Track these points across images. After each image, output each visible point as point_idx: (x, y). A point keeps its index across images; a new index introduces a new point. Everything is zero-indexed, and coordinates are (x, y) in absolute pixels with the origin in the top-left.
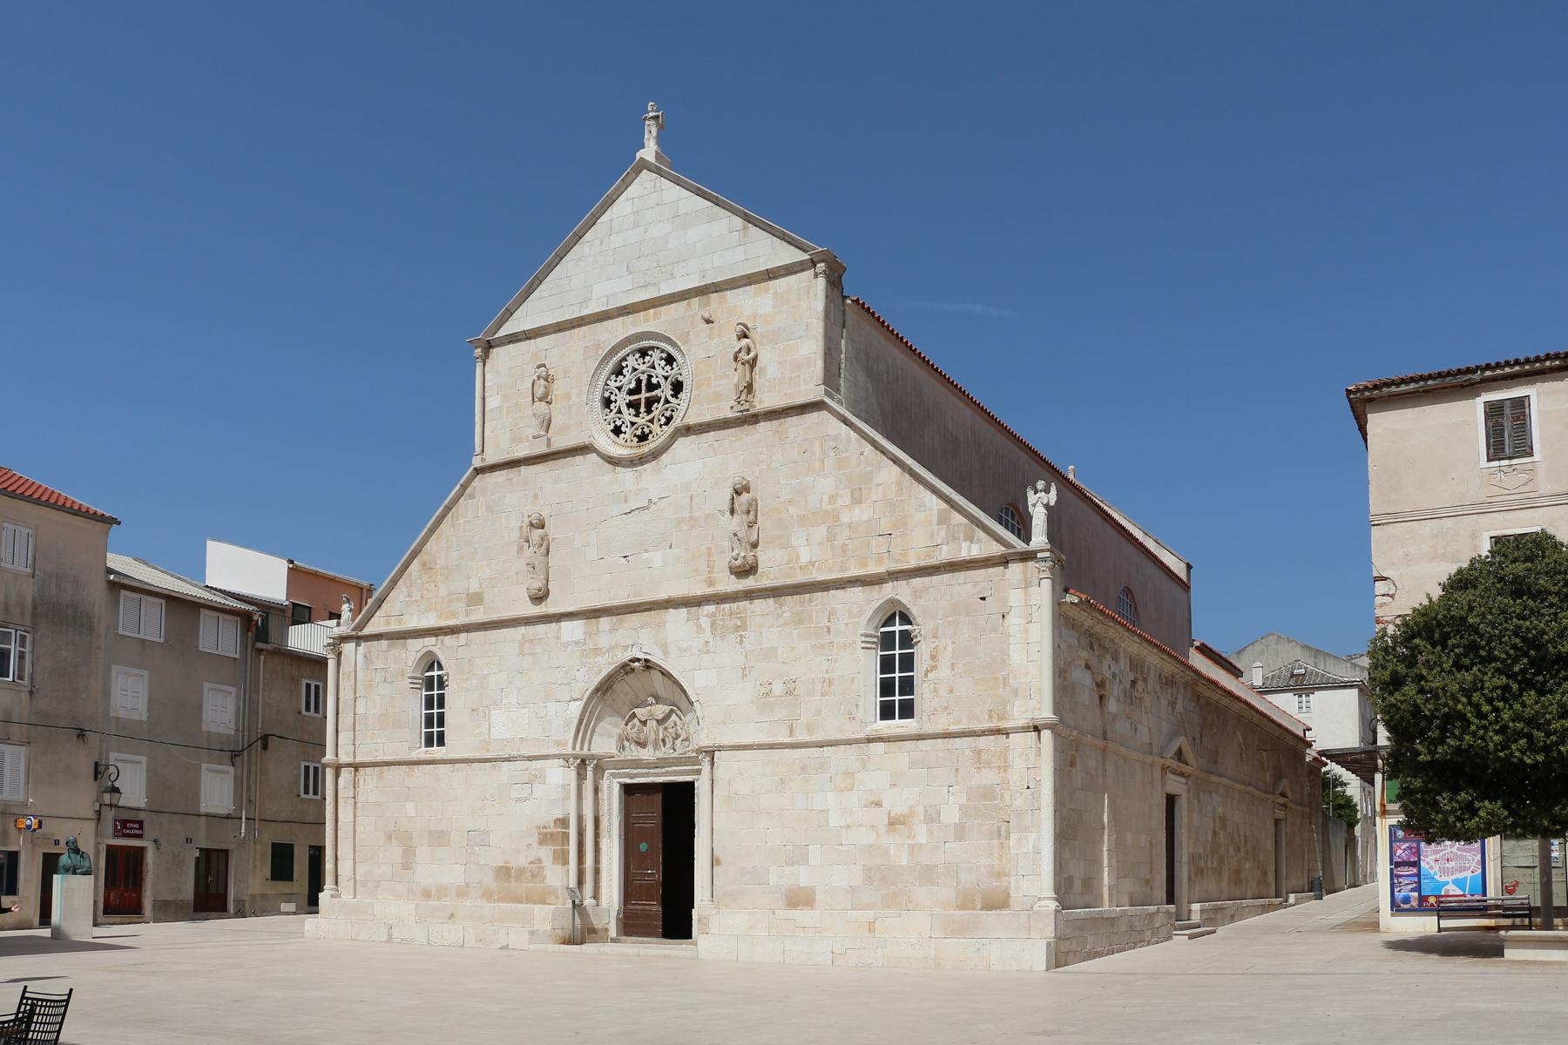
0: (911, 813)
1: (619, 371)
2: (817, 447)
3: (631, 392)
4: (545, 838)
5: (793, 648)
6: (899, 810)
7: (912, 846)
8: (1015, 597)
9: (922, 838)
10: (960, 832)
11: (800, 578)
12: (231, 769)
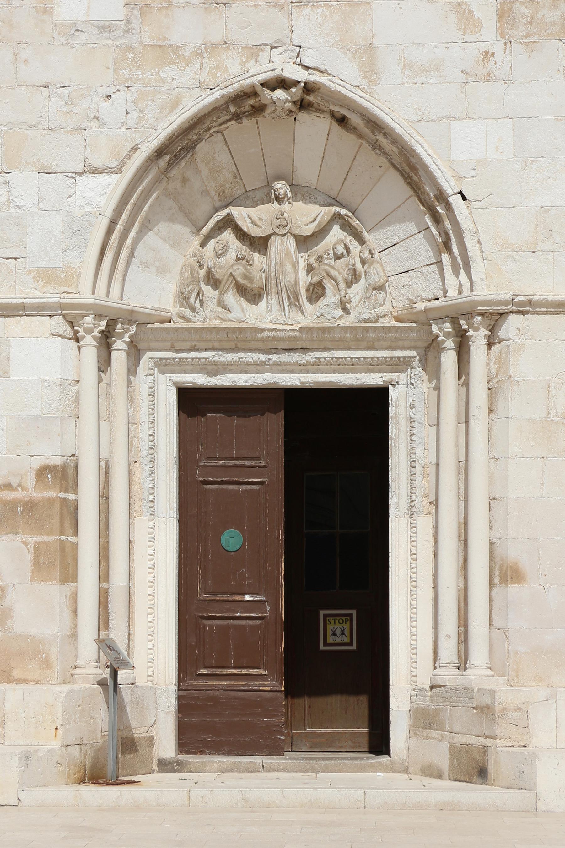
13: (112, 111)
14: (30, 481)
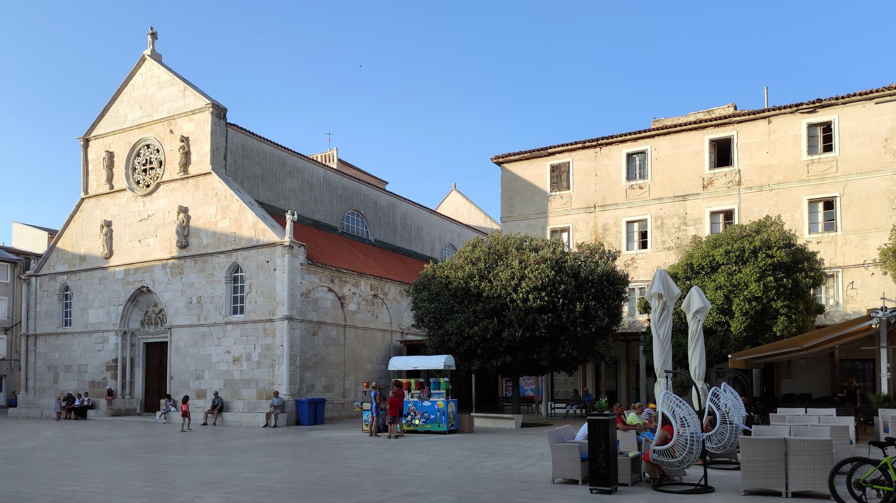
0: (241, 356)
1: (138, 155)
2: (210, 193)
3: (144, 165)
4: (109, 368)
6: (237, 355)
8: (279, 262)
9: (245, 367)
10: (259, 365)
11: (203, 252)
12: (5, 337)
13: (122, 294)
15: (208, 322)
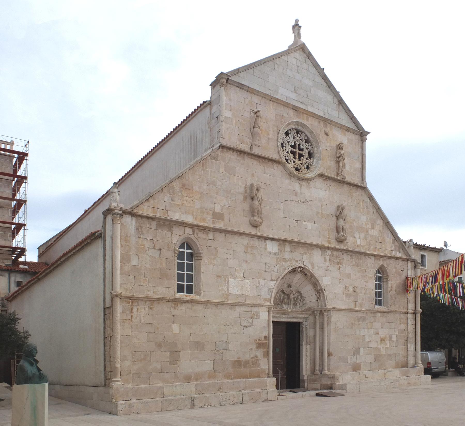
0: (386, 337)
4: (259, 345)
5: (355, 275)
6: (383, 336)
7: (386, 348)
9: (388, 346)
13: (276, 269)
14: (263, 339)
15: (363, 309)
